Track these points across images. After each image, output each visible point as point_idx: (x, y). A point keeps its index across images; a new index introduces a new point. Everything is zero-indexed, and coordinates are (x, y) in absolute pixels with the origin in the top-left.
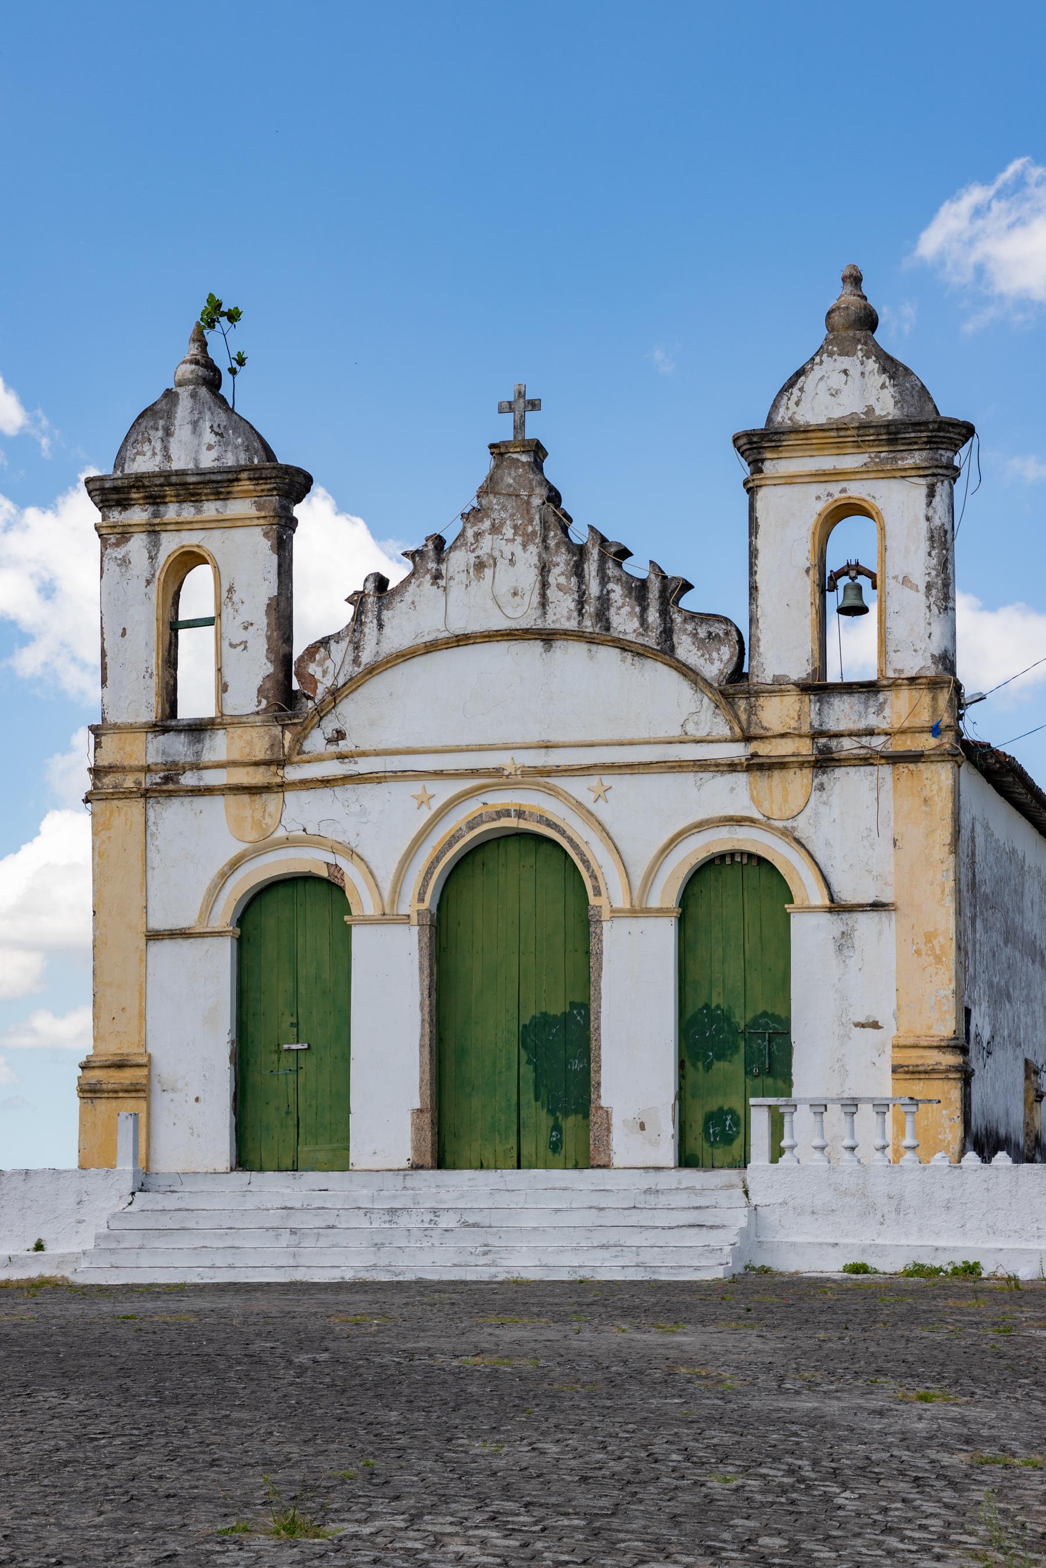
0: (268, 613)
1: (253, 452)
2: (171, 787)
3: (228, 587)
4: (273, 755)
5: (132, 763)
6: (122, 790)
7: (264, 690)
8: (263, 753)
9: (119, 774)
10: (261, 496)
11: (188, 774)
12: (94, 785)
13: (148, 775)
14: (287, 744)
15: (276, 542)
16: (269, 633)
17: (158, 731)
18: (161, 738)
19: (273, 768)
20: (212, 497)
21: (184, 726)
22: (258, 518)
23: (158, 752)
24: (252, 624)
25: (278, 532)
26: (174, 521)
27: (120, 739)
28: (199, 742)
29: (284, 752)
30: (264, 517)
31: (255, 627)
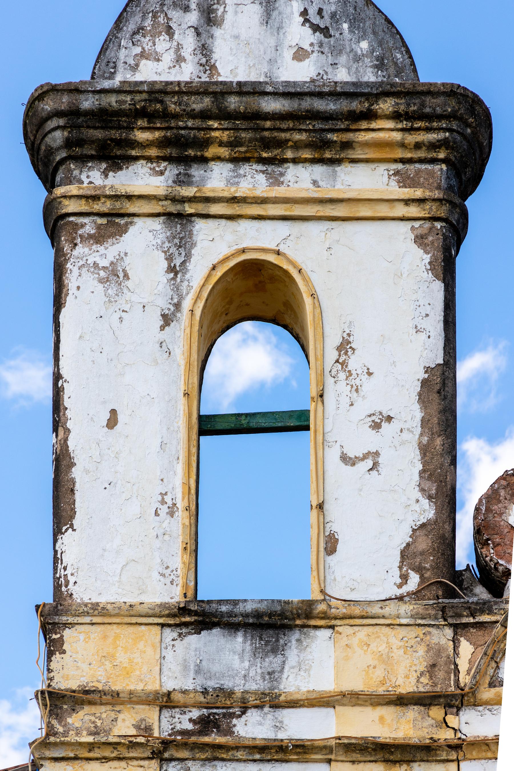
0: (422, 398)
1: (392, 70)
2: (214, 738)
3: (338, 341)
4: (435, 685)
5: (132, 687)
6: (112, 739)
7: (415, 554)
8: (413, 680)
9: (103, 708)
10: (410, 161)
11: (253, 715)
12: (50, 726)
13: (166, 713)
14: (463, 665)
15: (440, 255)
16: (425, 440)
17: (186, 624)
18: (194, 638)
19: (437, 712)
20: (307, 154)
21: (246, 615)
22: (407, 202)
23: (185, 668)
24: (389, 419)
25: (445, 238)
26: (226, 194)
27: (105, 637)
28: (275, 651)
29: (457, 681)
30: (421, 201)
31: (395, 425)
